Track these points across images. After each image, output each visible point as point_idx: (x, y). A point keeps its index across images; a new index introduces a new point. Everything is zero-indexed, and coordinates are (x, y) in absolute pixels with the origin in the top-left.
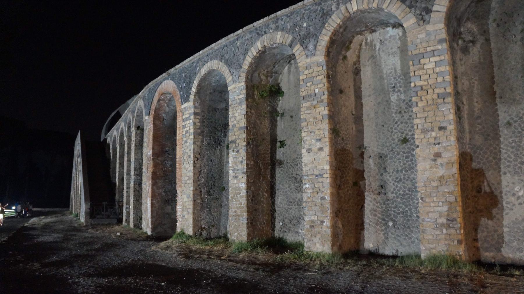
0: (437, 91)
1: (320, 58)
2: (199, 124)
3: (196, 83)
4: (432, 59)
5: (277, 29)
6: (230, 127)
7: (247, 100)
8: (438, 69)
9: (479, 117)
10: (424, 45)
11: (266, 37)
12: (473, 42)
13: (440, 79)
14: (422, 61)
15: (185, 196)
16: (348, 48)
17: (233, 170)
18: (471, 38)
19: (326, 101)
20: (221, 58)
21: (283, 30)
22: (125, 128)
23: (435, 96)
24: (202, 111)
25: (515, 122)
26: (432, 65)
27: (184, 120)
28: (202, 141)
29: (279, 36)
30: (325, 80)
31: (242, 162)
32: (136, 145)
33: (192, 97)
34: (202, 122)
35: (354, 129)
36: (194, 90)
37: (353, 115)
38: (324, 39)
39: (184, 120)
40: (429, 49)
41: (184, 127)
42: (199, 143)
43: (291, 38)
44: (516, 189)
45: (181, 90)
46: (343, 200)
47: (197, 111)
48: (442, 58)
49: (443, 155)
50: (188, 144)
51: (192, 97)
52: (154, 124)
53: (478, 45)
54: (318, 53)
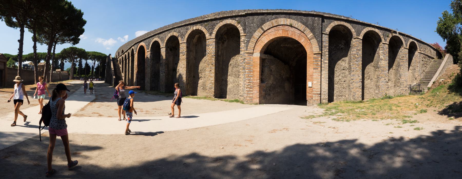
0: (212, 54)
2: (152, 57)
4: (211, 46)
5: (174, 31)
6: (161, 59)
7: (166, 51)
8: (212, 49)
9: (224, 61)
10: (210, 42)
11: (172, 33)
12: (225, 41)
13: (213, 52)
14: (209, 46)
15: (148, 78)
16: (194, 38)
17: (161, 72)
18: (225, 40)
19: (186, 54)
20: (159, 37)
21: (176, 32)
23: (211, 56)
24: (153, 53)
25: (232, 63)
26: (211, 48)
28: (153, 62)
29: (175, 34)
30: (186, 48)
31: (164, 69)
34: (153, 56)
35: (195, 61)
37: (194, 57)
38: (186, 36)
40: (211, 43)
43: (178, 34)
44: (231, 80)
45: (146, 45)
46: (190, 81)
48: (214, 46)
49: (212, 71)
50: (149, 63)
51: (150, 48)
53: (226, 42)
54: (185, 40)
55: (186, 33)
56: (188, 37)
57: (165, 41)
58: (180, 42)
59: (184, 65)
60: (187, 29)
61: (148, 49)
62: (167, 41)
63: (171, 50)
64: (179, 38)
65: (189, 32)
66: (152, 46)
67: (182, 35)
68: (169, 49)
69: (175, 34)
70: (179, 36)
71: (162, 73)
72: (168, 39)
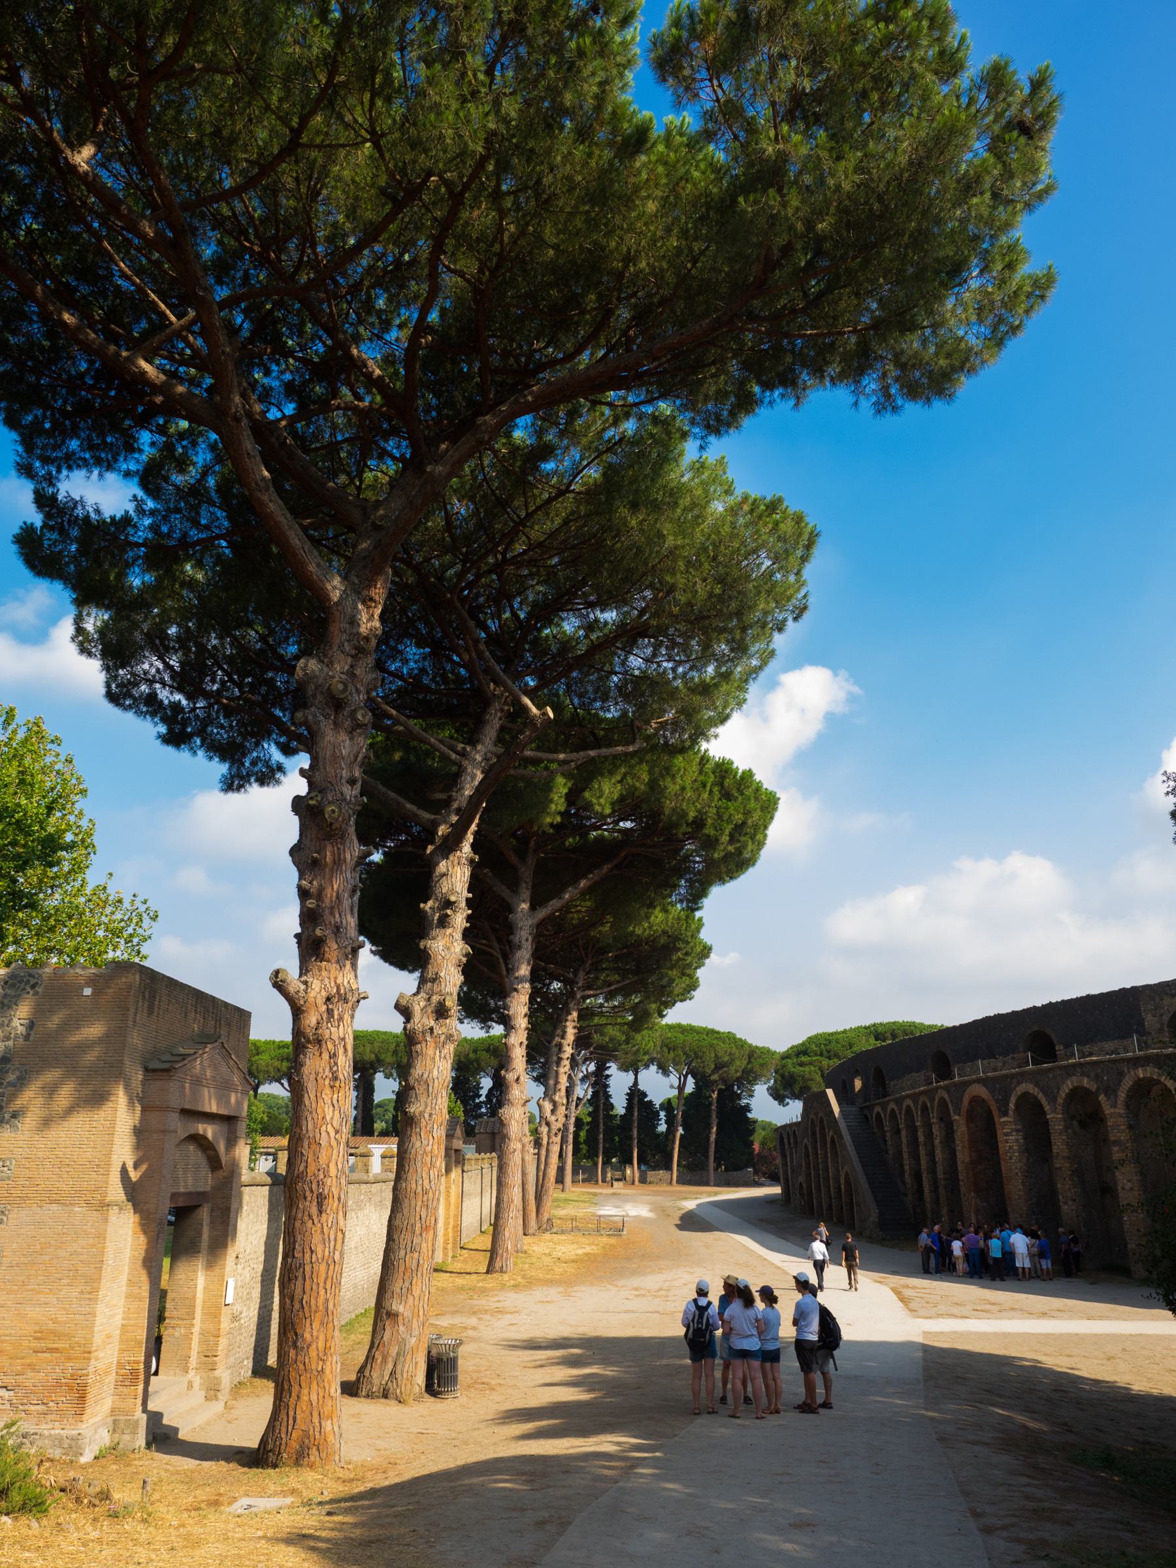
1: (1120, 1110)
3: (1013, 1099)
5: (1083, 1074)
11: (1074, 1078)
20: (1037, 1084)
21: (1088, 1076)
22: (916, 1108)
27: (1007, 1134)
32: (941, 1142)
33: (1011, 1113)
34: (1025, 1138)
36: (1012, 1106)
38: (1122, 1095)
39: (1007, 1134)
41: (1007, 1141)
42: (1025, 1161)
45: (997, 1101)
47: (1019, 1127)
52: (968, 1127)
55: (1119, 1084)
56: (1129, 1097)
57: (1060, 1101)
58: (1108, 1110)
59: (1129, 1181)
60: (1121, 1074)
61: (1006, 1114)
62: (1065, 1100)
63: (1083, 1125)
64: (1102, 1098)
65: (1127, 1083)
66: (1017, 1105)
67: (1111, 1091)
68: (1075, 1123)
69: (1085, 1082)
70: (1098, 1089)
71: (1066, 1204)
72: (1068, 1095)
